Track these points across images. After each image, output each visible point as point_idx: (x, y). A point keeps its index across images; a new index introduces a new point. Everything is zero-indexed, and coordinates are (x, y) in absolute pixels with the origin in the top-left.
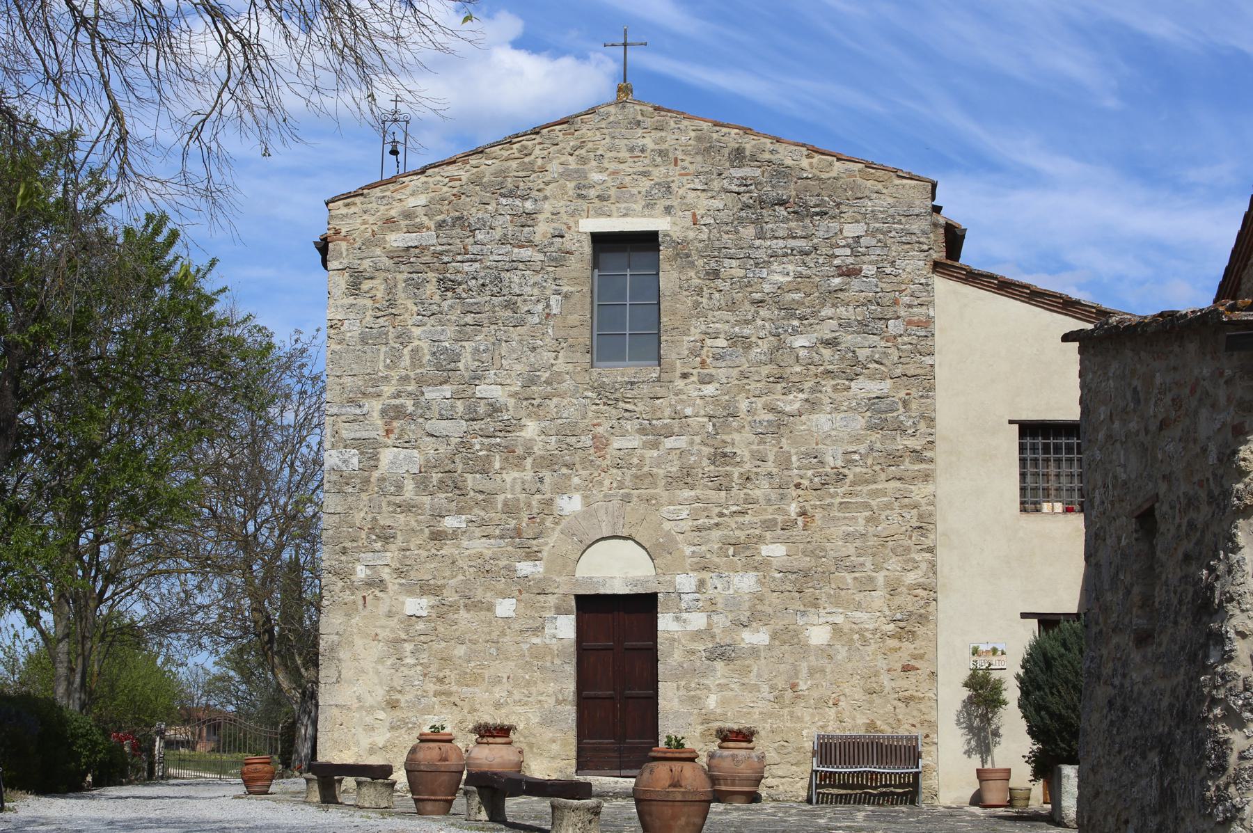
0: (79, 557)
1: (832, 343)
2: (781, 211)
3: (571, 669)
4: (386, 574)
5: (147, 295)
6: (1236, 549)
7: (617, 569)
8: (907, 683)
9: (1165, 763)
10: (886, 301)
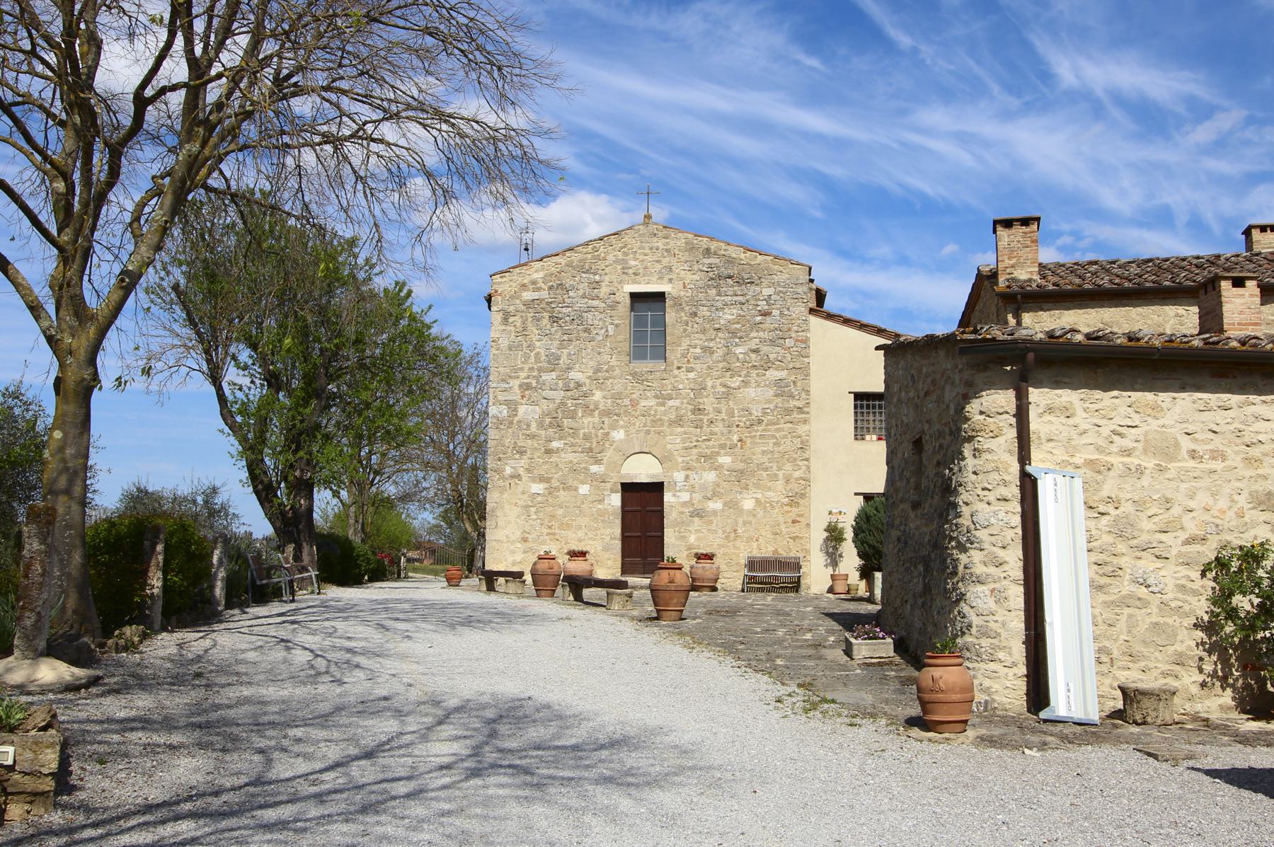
0: (360, 462)
1: (756, 351)
2: (729, 281)
3: (618, 522)
4: (521, 471)
5: (395, 324)
6: (963, 459)
7: (643, 470)
8: (795, 530)
9: (926, 570)
10: (785, 329)
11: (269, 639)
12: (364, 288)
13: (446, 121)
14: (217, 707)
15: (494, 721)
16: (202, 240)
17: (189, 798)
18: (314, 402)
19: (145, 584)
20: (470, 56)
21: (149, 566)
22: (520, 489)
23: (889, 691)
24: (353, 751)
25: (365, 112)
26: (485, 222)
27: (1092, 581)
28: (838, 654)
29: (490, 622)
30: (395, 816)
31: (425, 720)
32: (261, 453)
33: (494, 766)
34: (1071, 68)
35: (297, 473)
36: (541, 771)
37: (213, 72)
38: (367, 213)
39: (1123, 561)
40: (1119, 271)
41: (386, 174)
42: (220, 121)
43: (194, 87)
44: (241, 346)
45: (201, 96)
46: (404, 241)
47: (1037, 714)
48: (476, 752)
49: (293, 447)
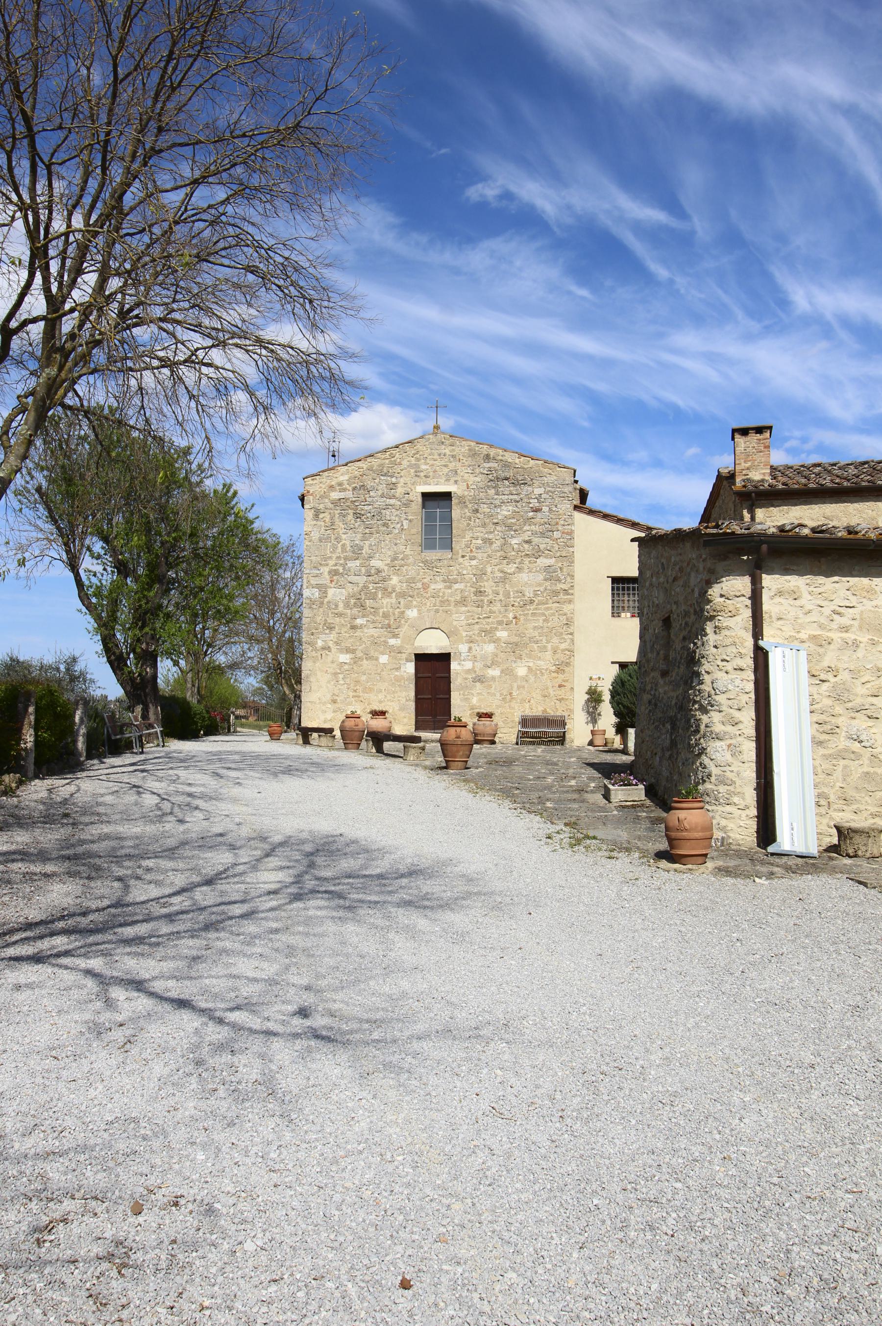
0: (196, 636)
1: (528, 542)
2: (506, 482)
4: (331, 644)
5: (224, 520)
6: (706, 635)
7: (433, 643)
8: (561, 693)
9: (673, 728)
11: (123, 785)
12: (198, 490)
13: (265, 348)
14: (82, 842)
15: (312, 854)
16: (62, 449)
17: (62, 918)
18: (157, 586)
19: (20, 739)
20: (286, 291)
21: (23, 725)
22: (330, 659)
23: (642, 829)
24: (196, 879)
25: (198, 340)
26: (297, 430)
27: (813, 738)
28: (598, 798)
29: (307, 770)
30: (232, 933)
31: (255, 853)
32: (113, 629)
33: (313, 891)
34: (805, 296)
35: (144, 646)
36: (352, 896)
37: (67, 307)
38: (199, 426)
39: (840, 721)
40: (839, 472)
41: (215, 393)
42: (74, 349)
43: (51, 319)
44: (95, 539)
45: (57, 327)
46: (230, 450)
47: (765, 849)
48: (298, 880)
49: (140, 624)
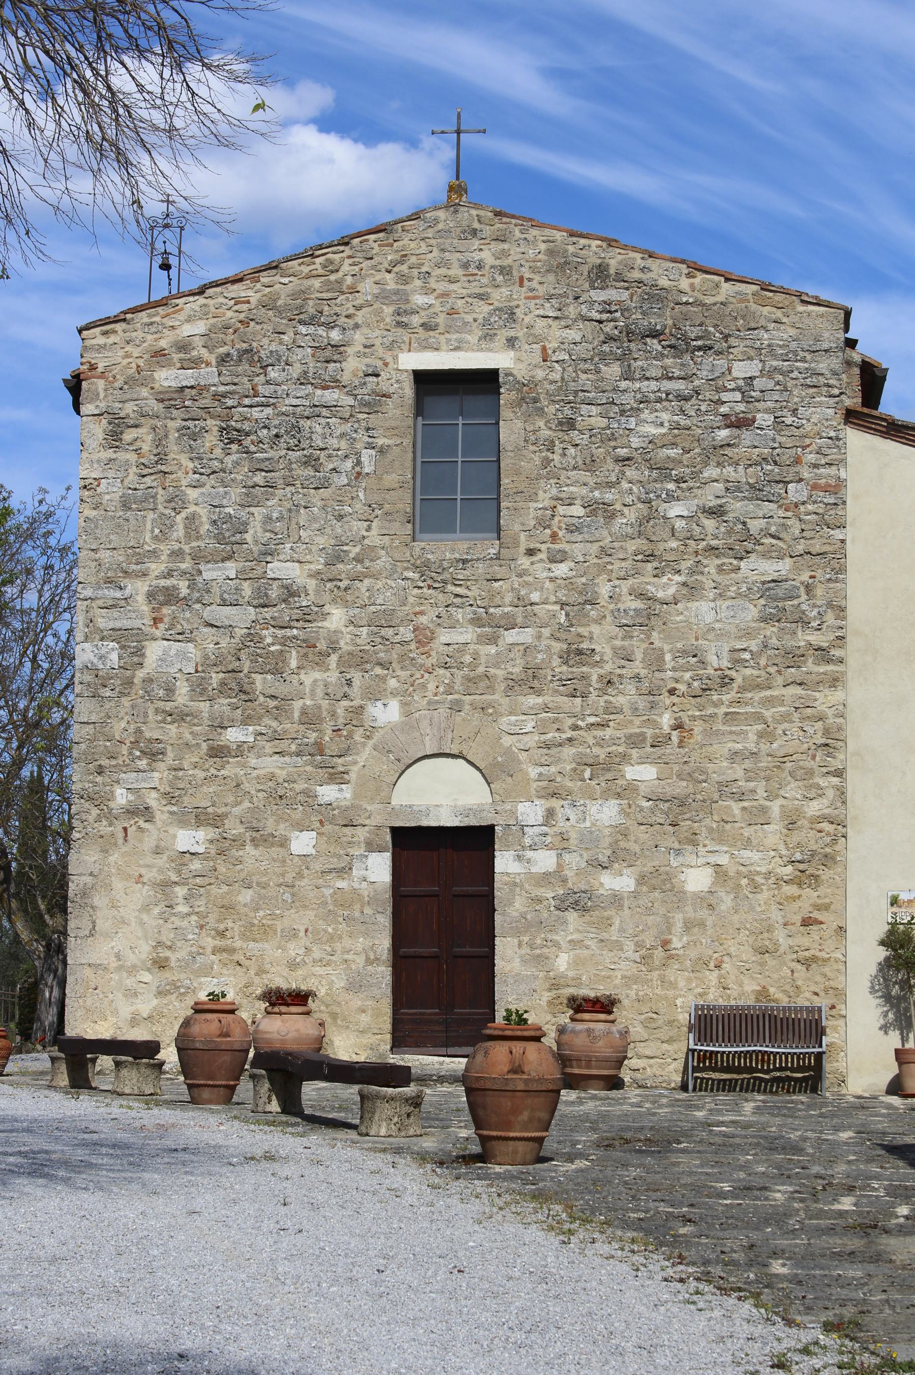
1: (717, 512)
3: (385, 921)
4: (152, 800)
7: (443, 795)
8: (809, 941)
10: (786, 459)
